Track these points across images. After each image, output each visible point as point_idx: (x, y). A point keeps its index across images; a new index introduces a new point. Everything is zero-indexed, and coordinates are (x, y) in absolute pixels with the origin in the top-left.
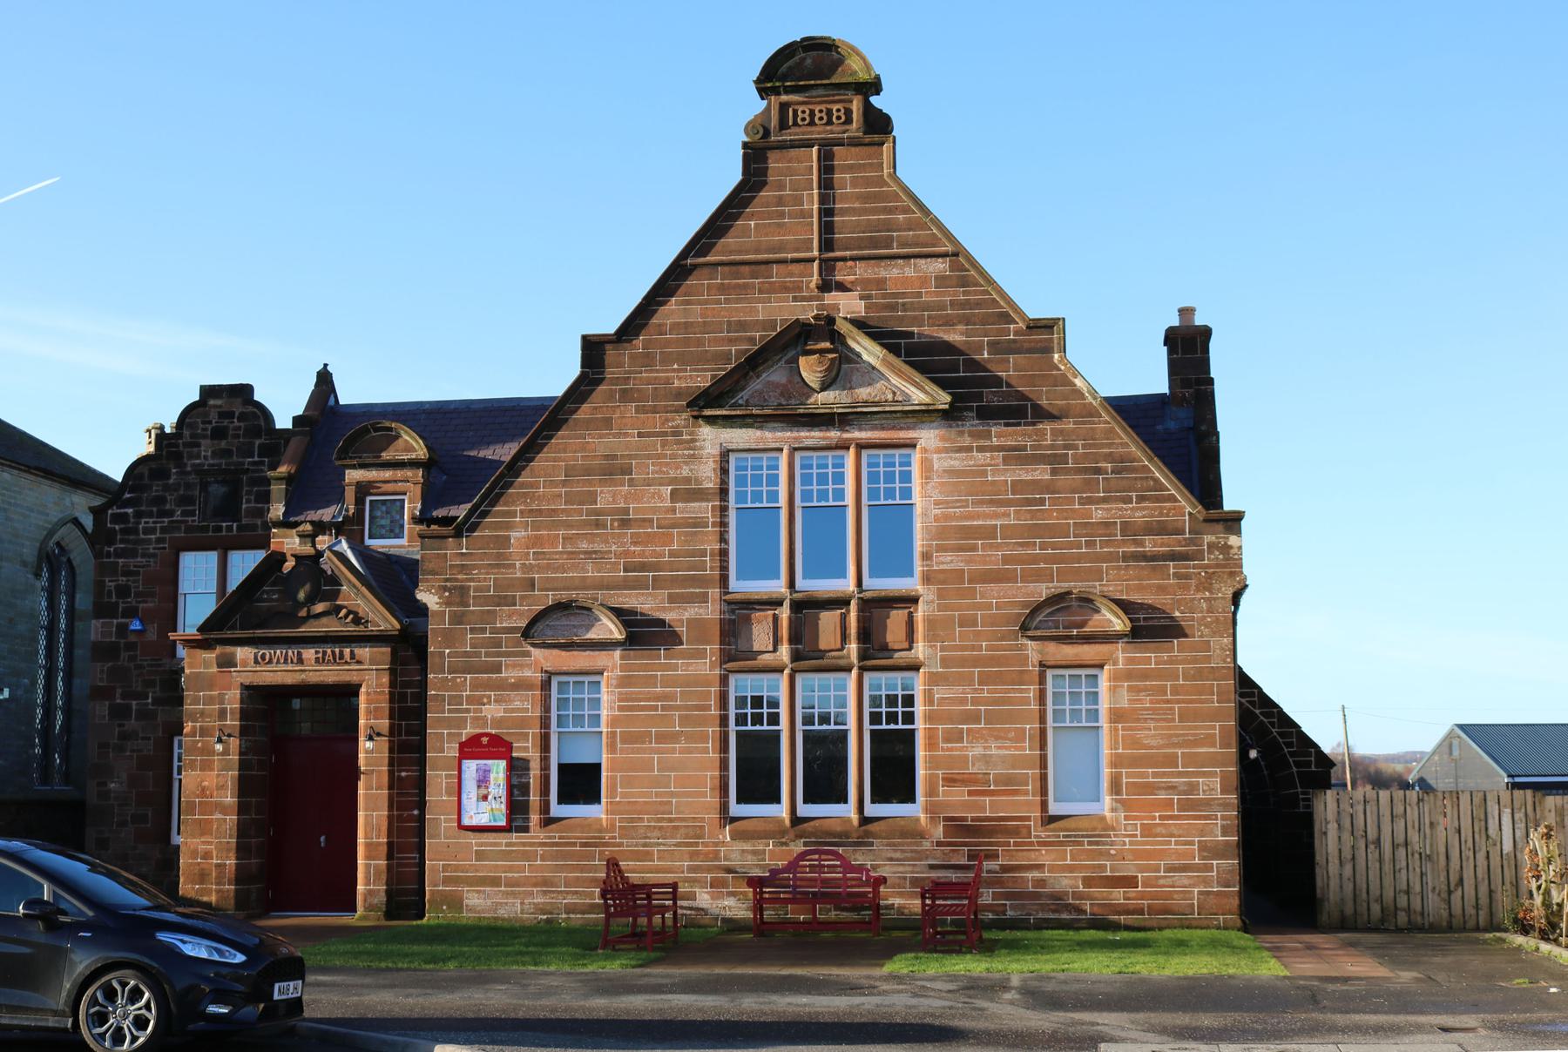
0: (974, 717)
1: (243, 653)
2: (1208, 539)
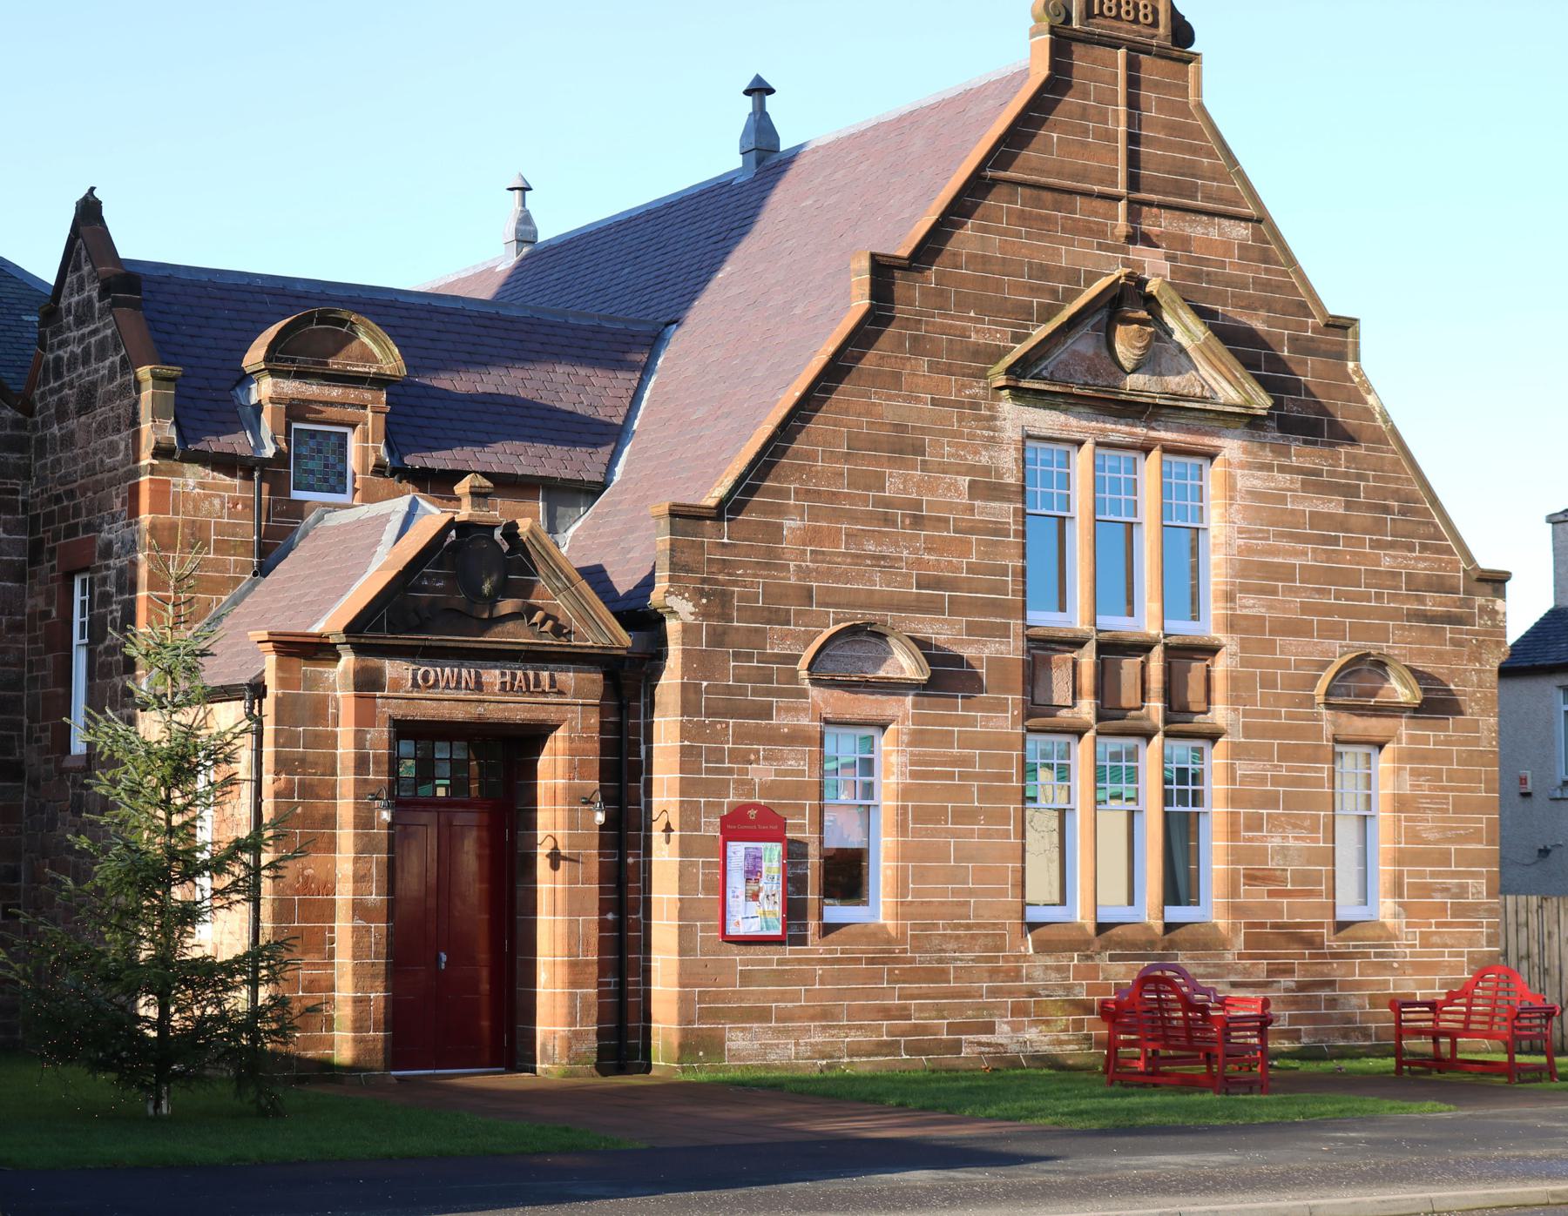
0: (1270, 801)
1: (395, 670)
2: (1479, 601)
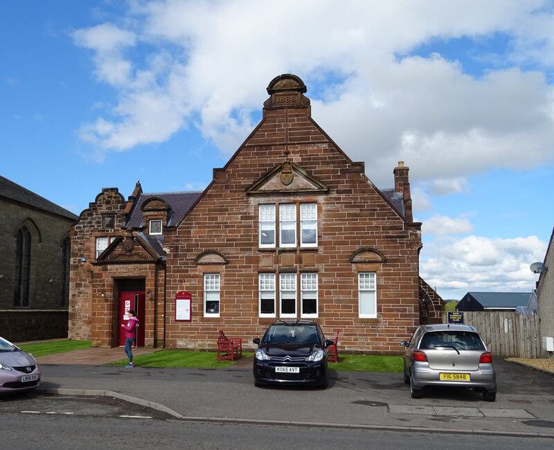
0: (335, 287)
